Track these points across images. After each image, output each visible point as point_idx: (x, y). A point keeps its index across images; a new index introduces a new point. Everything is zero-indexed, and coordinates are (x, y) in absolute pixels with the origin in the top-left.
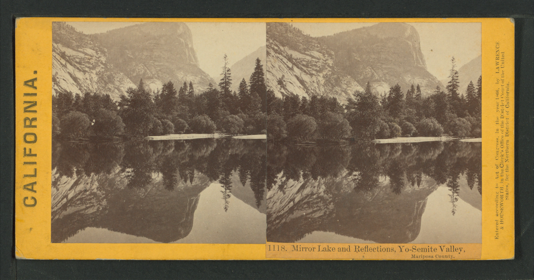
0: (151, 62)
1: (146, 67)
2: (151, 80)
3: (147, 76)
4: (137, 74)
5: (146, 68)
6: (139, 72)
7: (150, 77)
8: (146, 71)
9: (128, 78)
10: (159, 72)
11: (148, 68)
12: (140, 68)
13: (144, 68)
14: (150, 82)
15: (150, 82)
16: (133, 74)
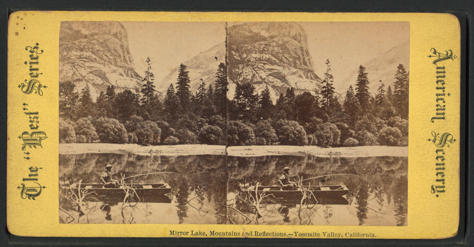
0: (260, 64)
1: (255, 70)
2: (260, 85)
3: (255, 80)
4: (244, 78)
5: (254, 72)
6: (246, 76)
7: (259, 81)
8: (254, 75)
9: (234, 82)
10: (270, 77)
11: (257, 71)
12: (247, 71)
13: (252, 71)
14: (259, 87)
15: (259, 87)
16: (240, 78)
